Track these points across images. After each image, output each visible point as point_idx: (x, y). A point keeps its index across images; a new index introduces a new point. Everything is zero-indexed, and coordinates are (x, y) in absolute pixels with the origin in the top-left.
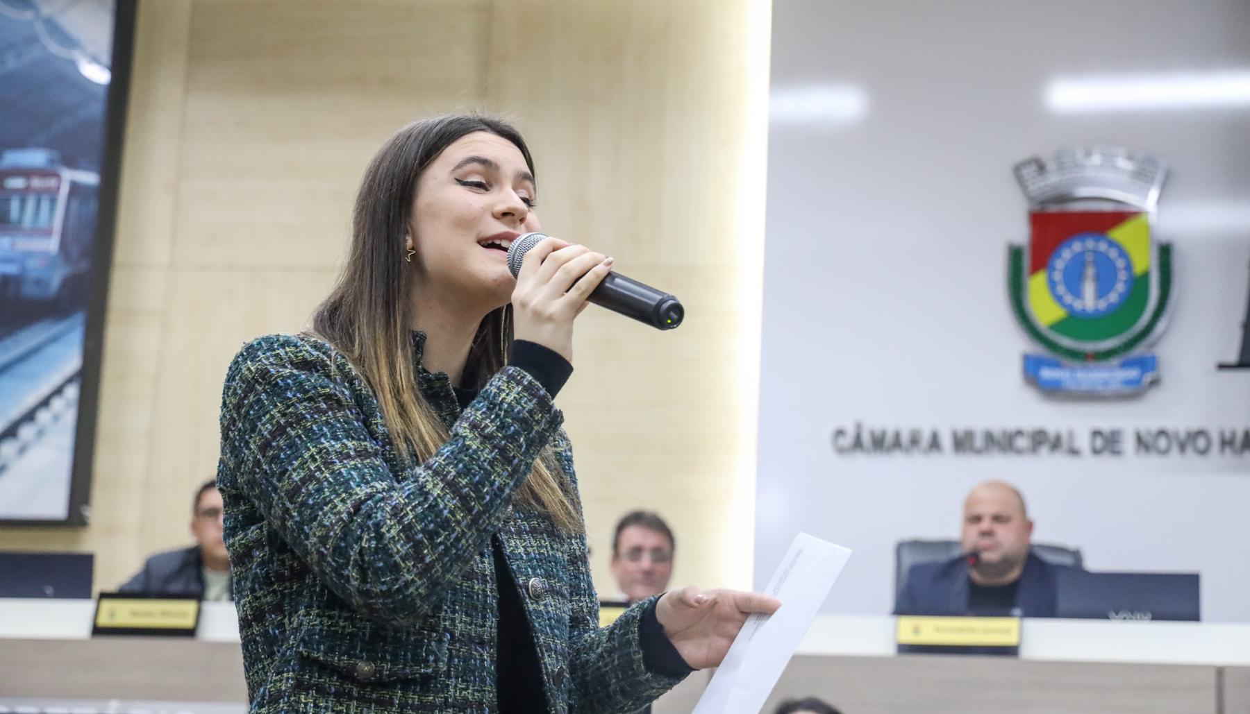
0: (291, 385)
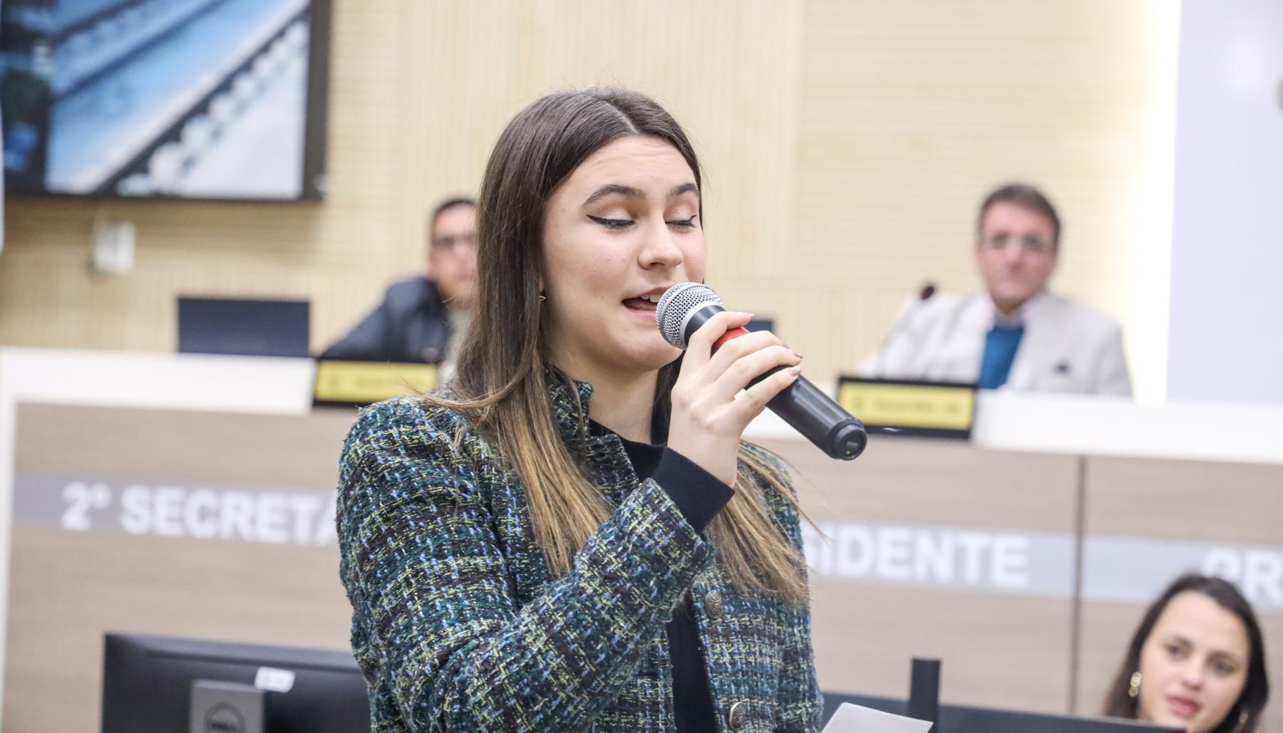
0: (399, 480)
